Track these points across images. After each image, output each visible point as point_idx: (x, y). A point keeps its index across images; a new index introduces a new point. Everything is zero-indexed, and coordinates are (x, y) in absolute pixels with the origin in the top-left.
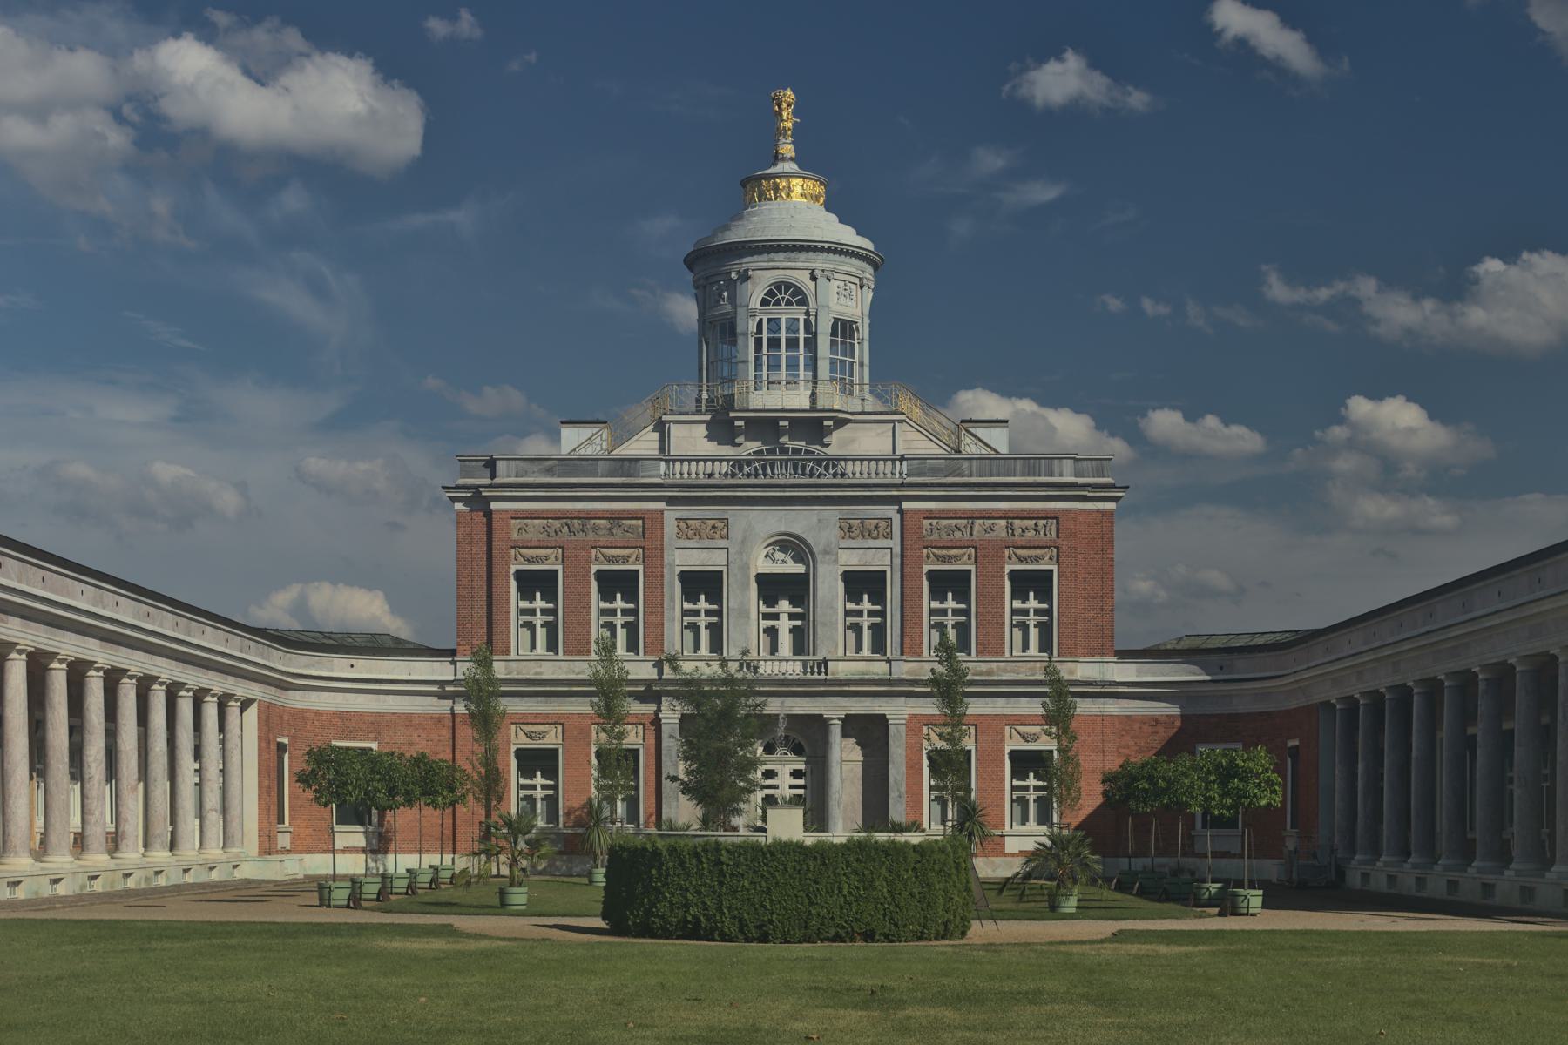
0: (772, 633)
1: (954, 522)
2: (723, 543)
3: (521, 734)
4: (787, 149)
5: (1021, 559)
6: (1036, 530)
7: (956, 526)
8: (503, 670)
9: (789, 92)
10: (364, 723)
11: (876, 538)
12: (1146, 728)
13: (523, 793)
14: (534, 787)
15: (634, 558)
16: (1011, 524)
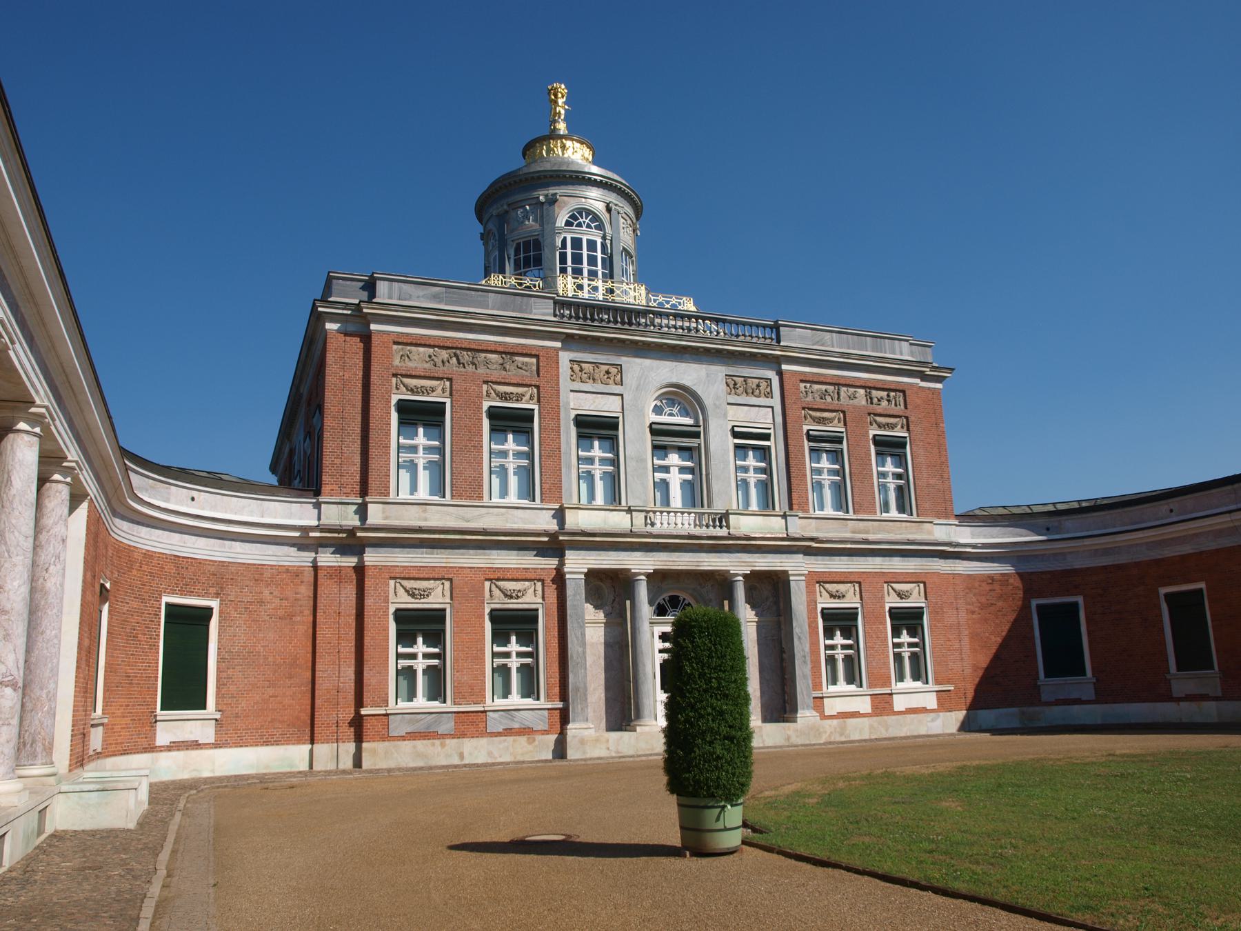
0: (664, 486)
1: (824, 387)
2: (617, 389)
3: (401, 591)
4: (562, 127)
5: (880, 426)
6: (889, 401)
7: (826, 391)
8: (380, 515)
9: (563, 86)
10: (204, 573)
11: (759, 396)
12: (984, 584)
13: (403, 663)
14: (413, 656)
15: (528, 396)
16: (870, 393)
